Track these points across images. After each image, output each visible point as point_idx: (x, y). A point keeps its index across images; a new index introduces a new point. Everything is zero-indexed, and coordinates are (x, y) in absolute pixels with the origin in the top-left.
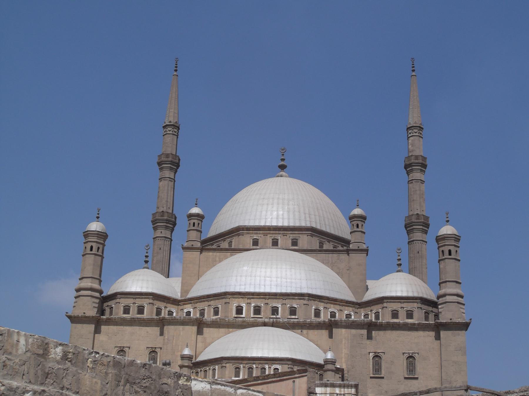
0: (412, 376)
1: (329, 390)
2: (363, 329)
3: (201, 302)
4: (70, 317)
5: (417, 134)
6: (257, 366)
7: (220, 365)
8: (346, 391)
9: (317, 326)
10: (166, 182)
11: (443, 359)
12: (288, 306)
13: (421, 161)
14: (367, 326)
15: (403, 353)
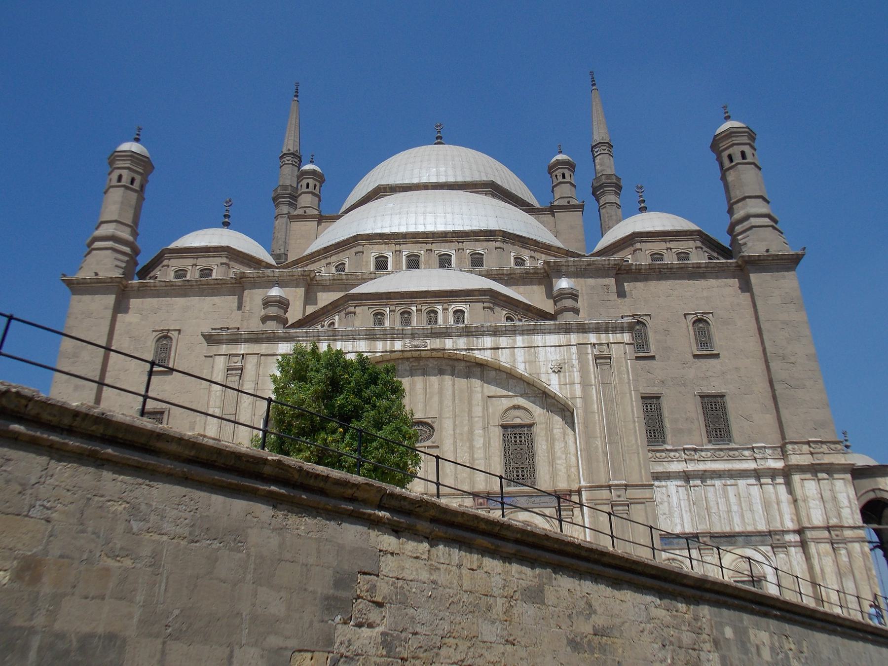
0: (708, 353)
1: (574, 338)
2: (608, 276)
3: (315, 262)
4: (69, 283)
5: (606, 152)
6: (419, 307)
7: (343, 314)
8: (611, 337)
9: (523, 278)
10: (285, 219)
11: (762, 318)
12: (468, 251)
13: (614, 181)
14: (615, 272)
15: (685, 315)
